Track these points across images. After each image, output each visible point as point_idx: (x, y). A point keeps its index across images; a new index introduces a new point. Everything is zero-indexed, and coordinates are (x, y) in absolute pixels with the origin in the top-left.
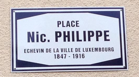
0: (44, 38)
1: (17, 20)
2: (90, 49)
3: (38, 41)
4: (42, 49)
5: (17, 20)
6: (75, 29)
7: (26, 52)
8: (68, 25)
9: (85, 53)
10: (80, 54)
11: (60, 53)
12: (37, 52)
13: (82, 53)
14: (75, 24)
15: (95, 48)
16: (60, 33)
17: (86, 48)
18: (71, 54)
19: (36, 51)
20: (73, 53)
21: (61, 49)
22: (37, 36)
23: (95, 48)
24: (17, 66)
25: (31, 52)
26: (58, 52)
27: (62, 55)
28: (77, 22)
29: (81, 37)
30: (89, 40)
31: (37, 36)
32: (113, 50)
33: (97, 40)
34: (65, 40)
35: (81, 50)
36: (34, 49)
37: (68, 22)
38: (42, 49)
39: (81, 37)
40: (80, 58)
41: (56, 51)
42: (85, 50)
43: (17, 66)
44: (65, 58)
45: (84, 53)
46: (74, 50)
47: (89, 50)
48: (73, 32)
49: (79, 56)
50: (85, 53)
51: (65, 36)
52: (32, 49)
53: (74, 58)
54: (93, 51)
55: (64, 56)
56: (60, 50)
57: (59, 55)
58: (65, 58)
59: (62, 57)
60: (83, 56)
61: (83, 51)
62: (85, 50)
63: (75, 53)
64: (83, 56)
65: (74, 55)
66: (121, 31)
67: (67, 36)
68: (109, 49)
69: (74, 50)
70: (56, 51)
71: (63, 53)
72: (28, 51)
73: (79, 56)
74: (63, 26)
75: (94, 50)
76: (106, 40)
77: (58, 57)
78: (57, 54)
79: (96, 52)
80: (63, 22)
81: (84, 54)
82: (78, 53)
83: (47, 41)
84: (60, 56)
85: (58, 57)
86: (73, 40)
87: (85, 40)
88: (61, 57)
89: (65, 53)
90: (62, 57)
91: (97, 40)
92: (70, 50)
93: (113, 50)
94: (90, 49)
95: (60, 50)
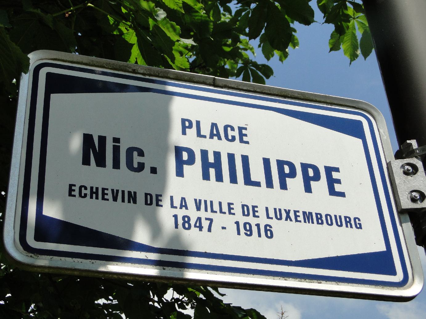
0: (137, 159)
1: (52, 96)
2: (288, 212)
3: (116, 165)
4: (133, 194)
5: (52, 96)
6: (237, 149)
7: (76, 193)
8: (214, 132)
9: (276, 225)
10: (258, 225)
11: (193, 213)
12: (115, 199)
13: (263, 221)
14: (236, 133)
15: (304, 213)
16: (191, 153)
17: (275, 209)
18: (229, 221)
19: (110, 196)
20: (234, 219)
21: (196, 200)
22: (116, 150)
23: (304, 213)
24: (38, 237)
25: (91, 197)
26: (184, 208)
27: (199, 219)
28: (240, 129)
29: (257, 174)
30: (284, 186)
31: (116, 150)
32: (358, 226)
33: (308, 189)
34: (206, 177)
35: (261, 212)
36: (103, 189)
37: (214, 125)
38: (129, 193)
39: (257, 174)
40: (260, 235)
41: (177, 203)
42: (272, 214)
43: (38, 237)
44: (209, 230)
45: (269, 222)
46: (237, 210)
47: (285, 215)
48: (231, 157)
49: (255, 229)
50: (276, 225)
51: (206, 166)
52: (97, 189)
53: (239, 233)
54: (299, 219)
55: (205, 224)
56: (191, 205)
57: (189, 219)
58: (209, 230)
59: (201, 228)
60: (269, 233)
61: (268, 217)
62: (272, 214)
63: (243, 220)
64: (269, 233)
65: (237, 223)
66: (374, 174)
67: (212, 166)
68: (348, 221)
69: (237, 210)
70: (177, 203)
71: (203, 214)
72: (84, 191)
73: (255, 229)
74: (199, 135)
75: (301, 218)
76: (332, 192)
77: (187, 225)
78: (181, 213)
79: (309, 225)
80: (198, 123)
81: (270, 227)
82: (251, 219)
83: (147, 169)
84: (192, 222)
85: (187, 225)
86: (234, 179)
87: (270, 184)
88: (195, 226)
89: (209, 215)
90: (198, 225)
91: (308, 189)
92: (225, 208)
93: (360, 224)
94: (288, 212)
95: (191, 205)
